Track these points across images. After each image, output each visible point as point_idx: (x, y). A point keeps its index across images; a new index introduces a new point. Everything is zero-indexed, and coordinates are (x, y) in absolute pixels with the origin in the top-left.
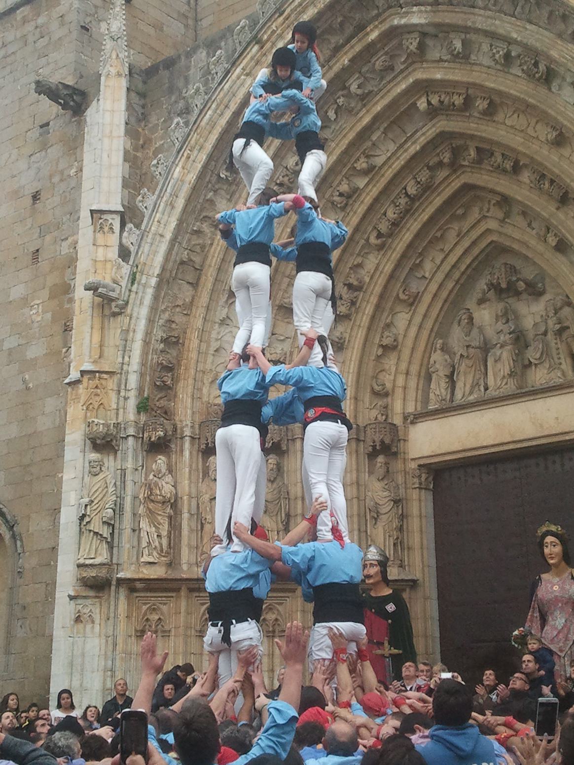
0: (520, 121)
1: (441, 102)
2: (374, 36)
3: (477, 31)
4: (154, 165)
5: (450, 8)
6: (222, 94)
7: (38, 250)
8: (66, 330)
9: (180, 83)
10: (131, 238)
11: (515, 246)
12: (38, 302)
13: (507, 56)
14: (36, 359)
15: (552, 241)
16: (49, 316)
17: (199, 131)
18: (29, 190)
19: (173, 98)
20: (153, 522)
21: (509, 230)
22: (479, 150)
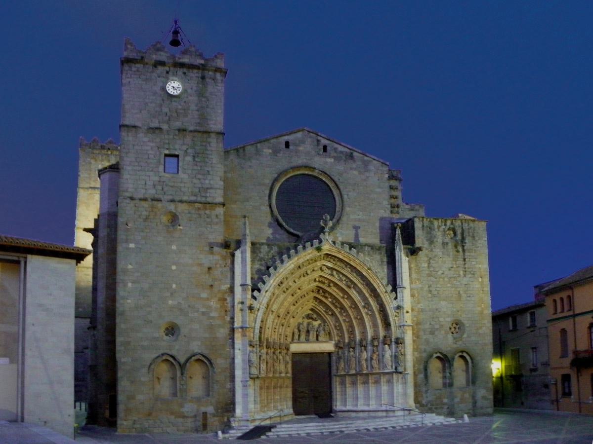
3: (341, 273)
7: (212, 285)
9: (258, 252)
10: (256, 293)
18: (207, 265)
19: (255, 255)
20: (263, 365)
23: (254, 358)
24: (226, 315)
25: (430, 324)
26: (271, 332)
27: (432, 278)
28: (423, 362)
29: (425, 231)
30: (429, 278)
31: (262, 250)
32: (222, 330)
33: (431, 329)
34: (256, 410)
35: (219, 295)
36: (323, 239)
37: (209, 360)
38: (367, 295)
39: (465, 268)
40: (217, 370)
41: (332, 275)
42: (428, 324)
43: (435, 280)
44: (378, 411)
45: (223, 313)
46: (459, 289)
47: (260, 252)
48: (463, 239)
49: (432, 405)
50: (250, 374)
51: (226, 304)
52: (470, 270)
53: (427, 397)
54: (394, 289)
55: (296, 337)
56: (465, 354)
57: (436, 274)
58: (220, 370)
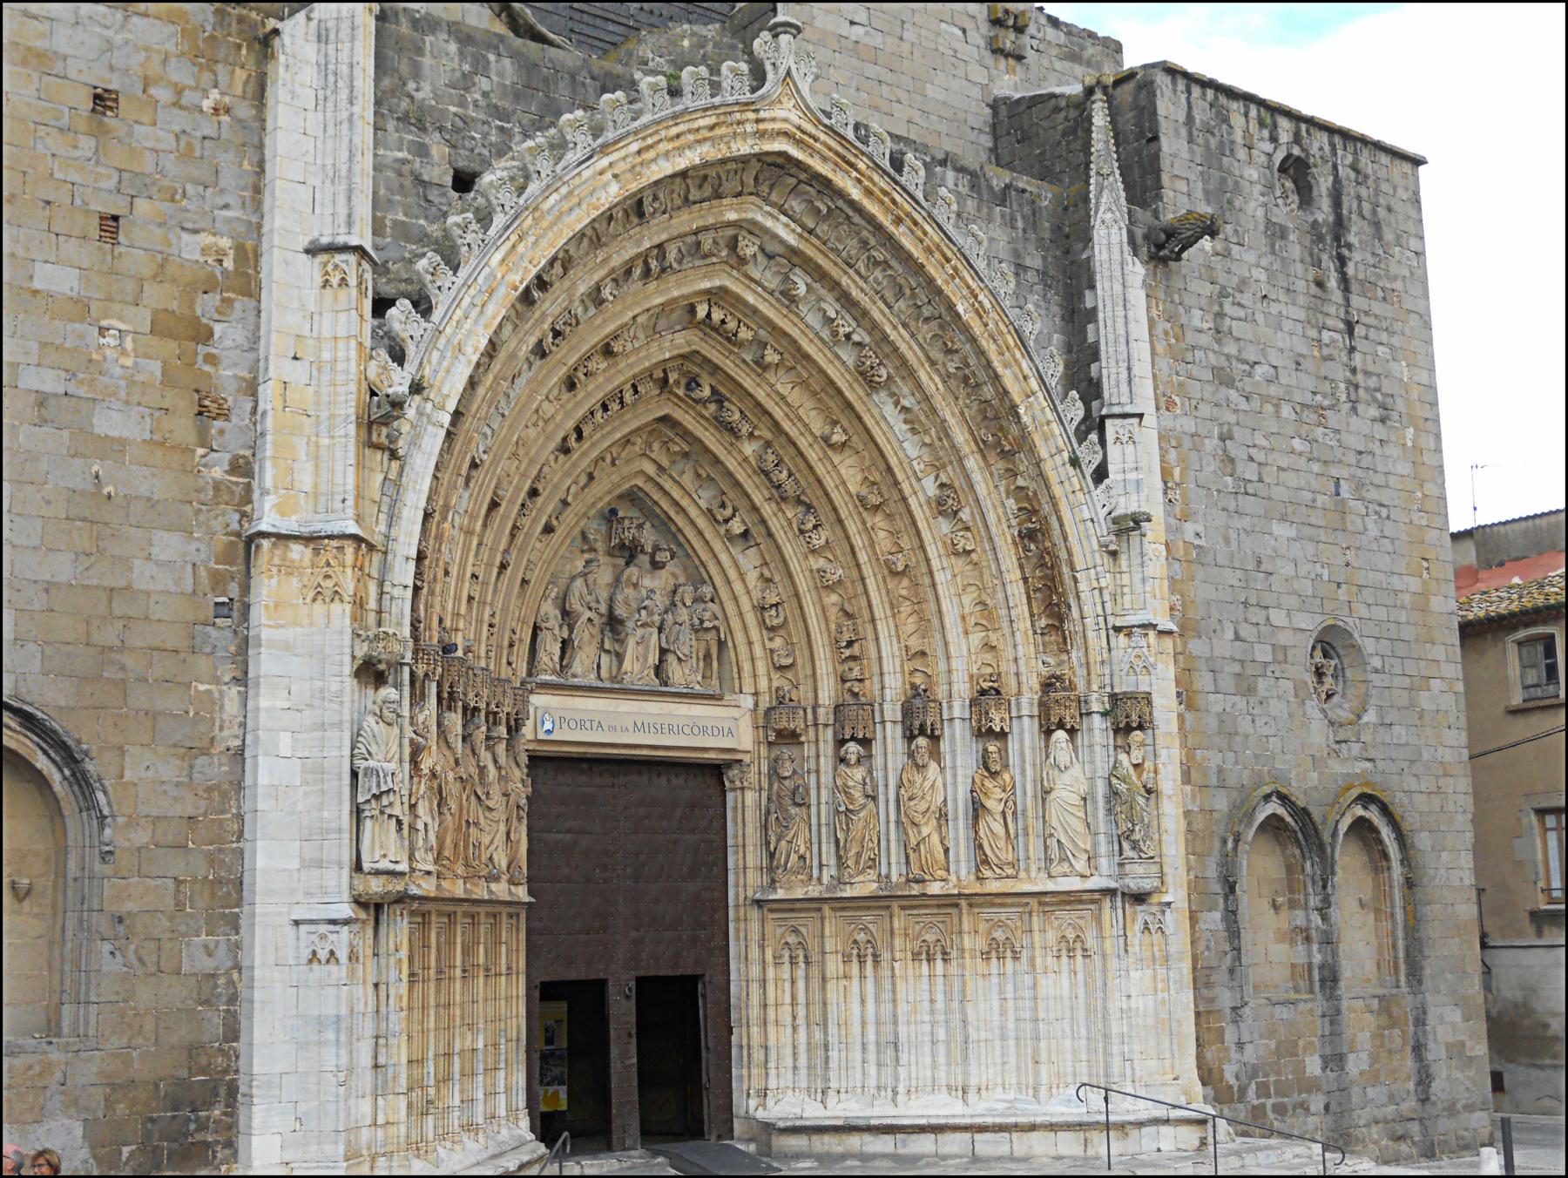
0: (795, 396)
1: (723, 322)
2: (732, 216)
3: (835, 285)
4: (458, 225)
5: (823, 247)
6: (577, 181)
7: (115, 218)
8: (200, 413)
11: (665, 505)
12: (123, 327)
13: (848, 336)
14: (123, 442)
15: (737, 527)
16: (156, 367)
17: (537, 214)
21: (668, 485)
22: (712, 388)
23: (387, 756)
24: (204, 441)
25: (1237, 638)
26: (457, 599)
27: (1232, 392)
28: (1217, 844)
29: (1198, 151)
30: (1224, 391)
31: (427, 61)
32: (168, 545)
33: (1242, 662)
34: (380, 1132)
35: (158, 296)
36: (768, 68)
37: (69, 757)
38: (960, 436)
39: (1354, 371)
40: (124, 837)
41: (788, 298)
42: (1230, 635)
43: (1243, 405)
44: (1033, 1127)
45: (182, 427)
46: (1335, 471)
47: (417, 74)
48: (1340, 224)
49: (1263, 1091)
50: (358, 867)
51: (207, 368)
52: (1372, 382)
53: (1240, 1045)
54: (1093, 425)
55: (550, 649)
56: (1373, 815)
57: (1250, 375)
58: (141, 837)
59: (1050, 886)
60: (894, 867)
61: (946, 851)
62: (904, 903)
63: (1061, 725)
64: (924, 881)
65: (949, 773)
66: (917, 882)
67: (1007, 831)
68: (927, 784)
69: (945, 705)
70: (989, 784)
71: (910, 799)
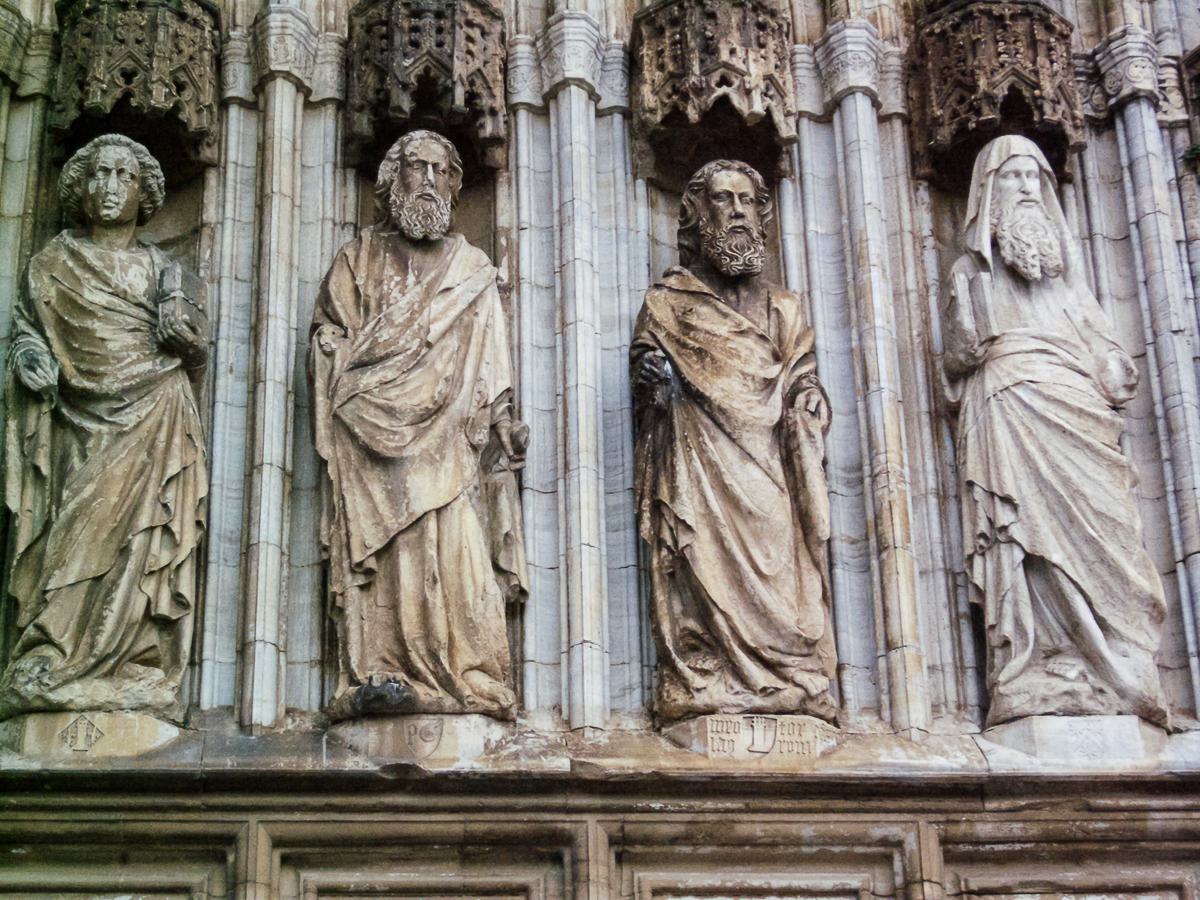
59: (1004, 756)
60: (264, 661)
61: (515, 608)
62: (305, 824)
63: (1018, 114)
64: (403, 709)
65: (532, 305)
66: (374, 707)
67: (804, 519)
68: (440, 314)
69: (523, 52)
70: (710, 320)
71: (361, 365)
